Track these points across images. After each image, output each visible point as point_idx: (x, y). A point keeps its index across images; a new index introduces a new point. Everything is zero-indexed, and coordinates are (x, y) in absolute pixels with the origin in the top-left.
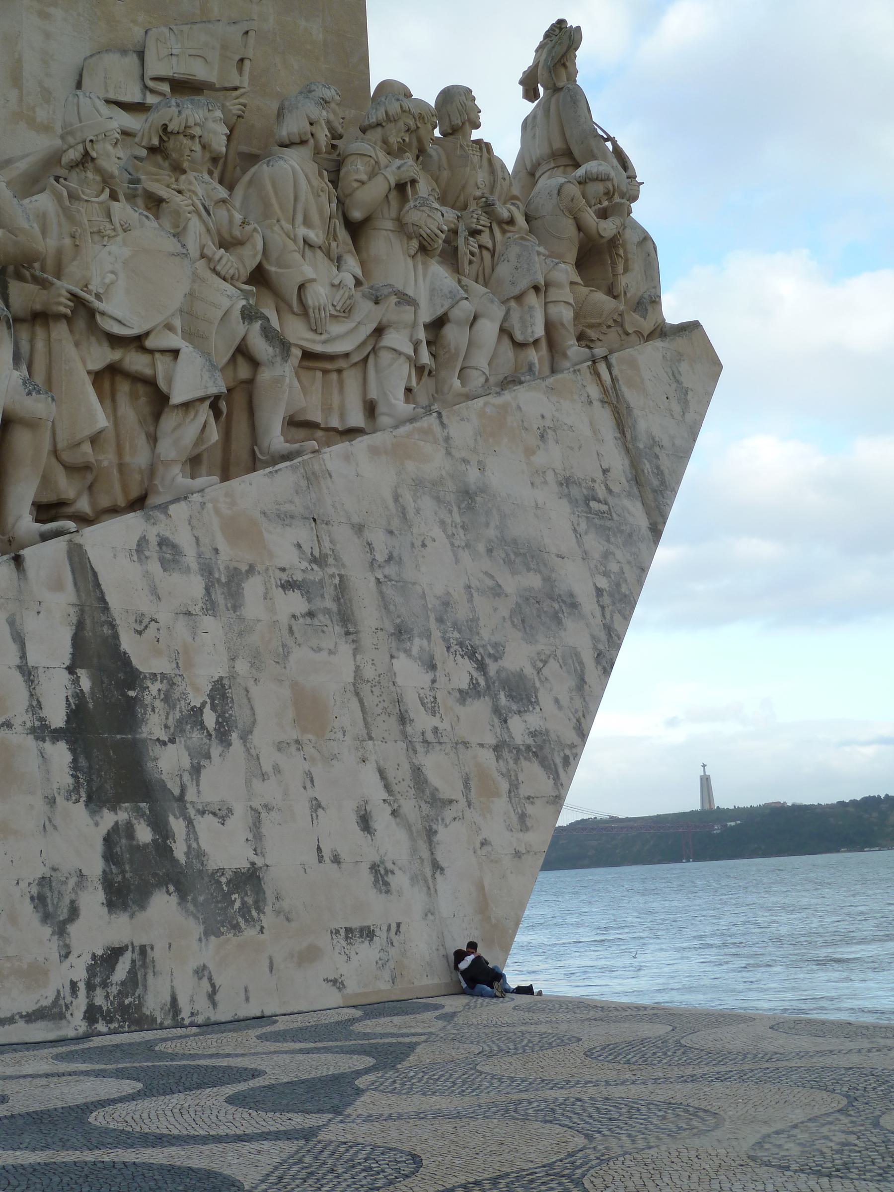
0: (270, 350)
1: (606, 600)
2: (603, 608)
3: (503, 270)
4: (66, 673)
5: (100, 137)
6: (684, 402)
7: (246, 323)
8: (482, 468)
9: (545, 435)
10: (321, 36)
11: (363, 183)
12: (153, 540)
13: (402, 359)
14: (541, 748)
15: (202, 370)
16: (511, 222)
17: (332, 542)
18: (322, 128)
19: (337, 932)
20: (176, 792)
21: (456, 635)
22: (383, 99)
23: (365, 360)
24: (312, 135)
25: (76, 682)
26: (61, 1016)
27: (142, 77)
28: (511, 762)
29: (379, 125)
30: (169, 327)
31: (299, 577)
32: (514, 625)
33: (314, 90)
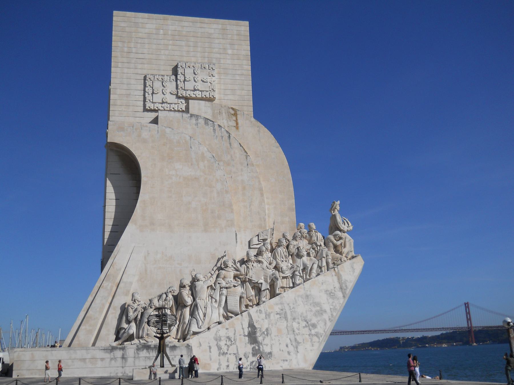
1: (332, 310)
2: (331, 311)
6: (354, 272)
8: (310, 291)
12: (259, 310)
14: (317, 334)
16: (321, 245)
17: (284, 307)
19: (282, 360)
20: (261, 342)
21: (304, 318)
25: (249, 329)
26: (247, 368)
28: (311, 337)
31: (279, 312)
32: (314, 316)
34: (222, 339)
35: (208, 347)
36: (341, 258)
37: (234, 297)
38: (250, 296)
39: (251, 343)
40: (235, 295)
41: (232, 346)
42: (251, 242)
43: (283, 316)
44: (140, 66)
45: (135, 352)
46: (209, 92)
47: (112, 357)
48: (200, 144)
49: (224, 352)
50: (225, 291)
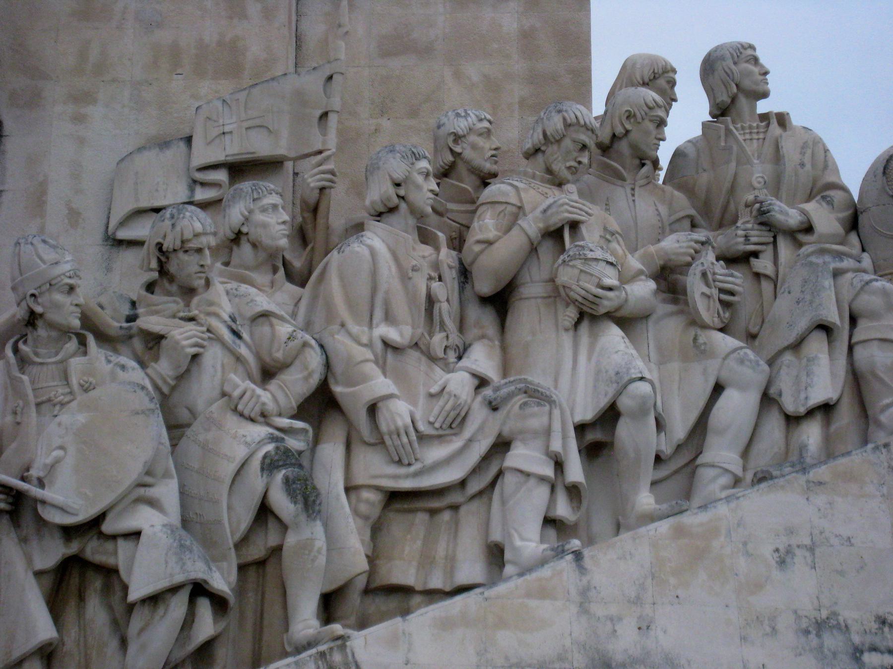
0: (292, 507)
3: (782, 306)
5: (44, 288)
7: (265, 476)
9: (788, 560)
10: (515, 25)
11: (489, 243)
13: (532, 482)
15: (166, 554)
16: (808, 229)
18: (419, 187)
22: (542, 114)
24: (398, 196)
27: (188, 170)
29: (537, 151)
30: (152, 503)
33: (444, 124)
38: (17, 654)
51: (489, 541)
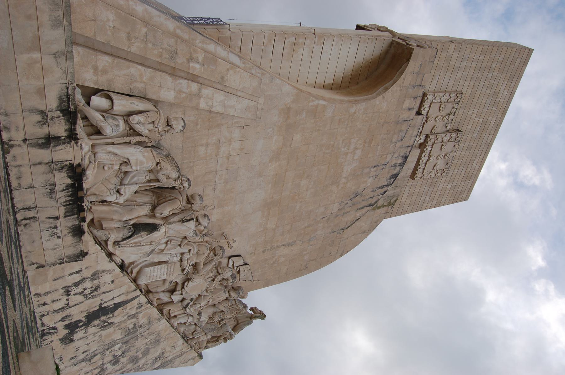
0: (185, 305)
4: (113, 303)
12: (141, 305)
13: (186, 321)
16: (220, 324)
23: (185, 313)
25: (112, 305)
29: (236, 304)
34: (96, 282)
35: (80, 269)
36: (202, 348)
37: (165, 274)
39: (87, 317)
40: (168, 274)
41: (84, 297)
42: (239, 257)
43: (131, 331)
44: (472, 84)
45: (66, 161)
46: (422, 172)
47: (49, 115)
48: (376, 177)
49: (71, 292)
50: (176, 259)
51: (177, 316)
